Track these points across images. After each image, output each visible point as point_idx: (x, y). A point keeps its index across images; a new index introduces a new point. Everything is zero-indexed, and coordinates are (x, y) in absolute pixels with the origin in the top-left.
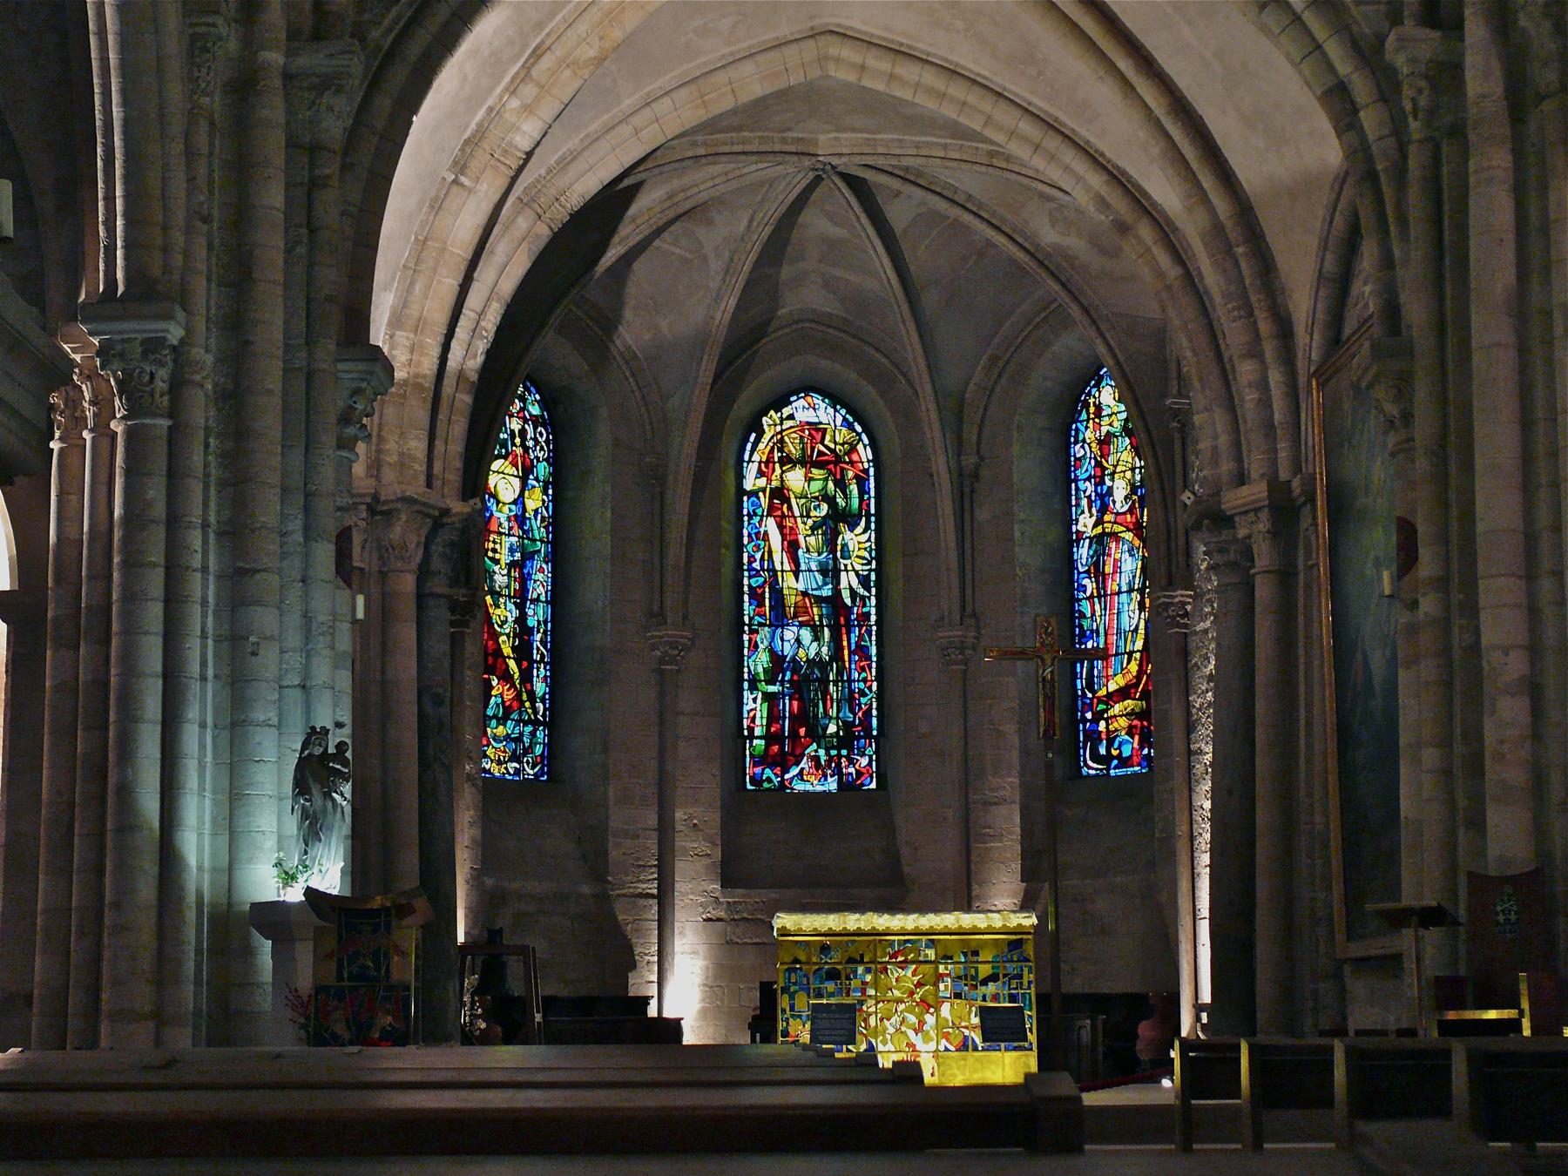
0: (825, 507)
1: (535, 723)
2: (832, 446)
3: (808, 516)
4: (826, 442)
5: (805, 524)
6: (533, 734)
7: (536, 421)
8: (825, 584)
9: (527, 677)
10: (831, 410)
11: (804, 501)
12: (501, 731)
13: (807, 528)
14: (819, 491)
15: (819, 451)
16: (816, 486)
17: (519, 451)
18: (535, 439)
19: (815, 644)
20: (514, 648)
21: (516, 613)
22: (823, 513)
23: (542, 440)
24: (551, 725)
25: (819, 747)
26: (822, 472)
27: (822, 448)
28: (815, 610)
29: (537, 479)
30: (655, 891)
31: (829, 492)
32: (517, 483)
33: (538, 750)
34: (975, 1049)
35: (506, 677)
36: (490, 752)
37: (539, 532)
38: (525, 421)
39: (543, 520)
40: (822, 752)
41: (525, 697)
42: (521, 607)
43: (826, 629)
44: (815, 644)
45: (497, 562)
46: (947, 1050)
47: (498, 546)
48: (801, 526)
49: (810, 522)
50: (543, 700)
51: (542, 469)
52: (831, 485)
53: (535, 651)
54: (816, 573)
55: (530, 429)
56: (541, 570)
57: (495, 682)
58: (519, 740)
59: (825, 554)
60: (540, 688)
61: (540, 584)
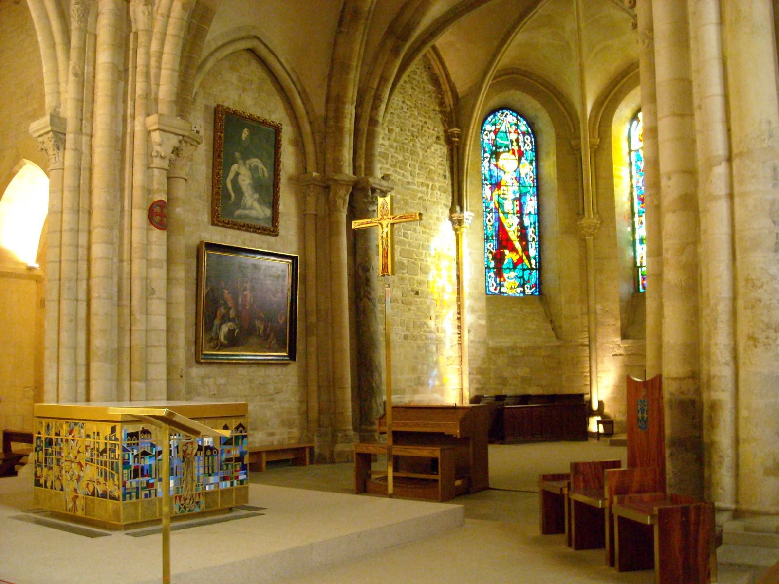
1: (532, 269)
6: (530, 274)
7: (524, 134)
9: (525, 249)
12: (513, 274)
17: (516, 148)
18: (525, 143)
20: (518, 237)
21: (518, 221)
23: (528, 142)
24: (540, 269)
29: (526, 159)
30: (587, 343)
32: (516, 162)
33: (533, 281)
34: (98, 496)
35: (513, 249)
36: (505, 284)
37: (529, 181)
38: (518, 134)
39: (531, 177)
41: (524, 258)
42: (521, 218)
45: (506, 199)
46: (88, 495)
47: (505, 192)
50: (535, 259)
51: (530, 155)
53: (529, 237)
55: (521, 138)
56: (531, 200)
57: (507, 252)
58: (523, 277)
60: (533, 252)
61: (531, 205)
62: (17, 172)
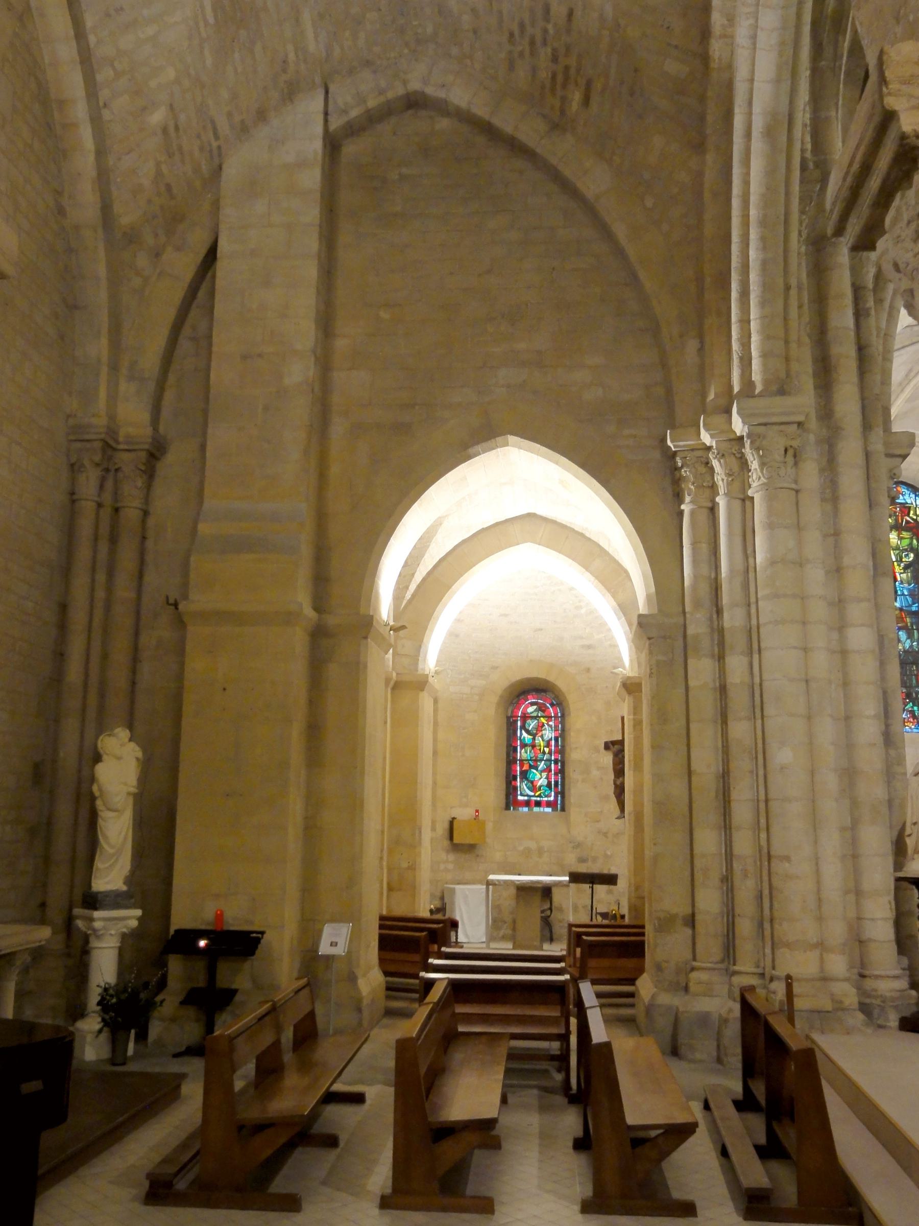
0: (912, 555)
2: (915, 517)
3: (901, 561)
4: (911, 515)
5: (899, 565)
8: (914, 603)
10: (913, 496)
11: (897, 552)
13: (901, 568)
14: (907, 546)
15: (906, 520)
16: (905, 543)
19: (909, 641)
22: (911, 559)
25: (914, 705)
26: (909, 533)
27: (908, 519)
28: (908, 620)
31: (914, 546)
40: (916, 708)
43: (915, 631)
44: (909, 641)
48: (897, 567)
49: (902, 565)
52: (915, 542)
54: (907, 597)
59: (913, 585)
62: (479, 454)
